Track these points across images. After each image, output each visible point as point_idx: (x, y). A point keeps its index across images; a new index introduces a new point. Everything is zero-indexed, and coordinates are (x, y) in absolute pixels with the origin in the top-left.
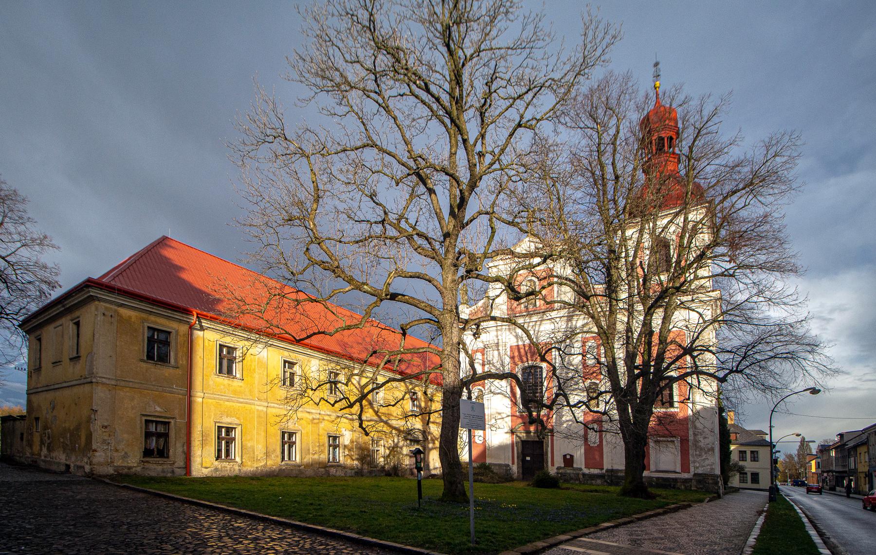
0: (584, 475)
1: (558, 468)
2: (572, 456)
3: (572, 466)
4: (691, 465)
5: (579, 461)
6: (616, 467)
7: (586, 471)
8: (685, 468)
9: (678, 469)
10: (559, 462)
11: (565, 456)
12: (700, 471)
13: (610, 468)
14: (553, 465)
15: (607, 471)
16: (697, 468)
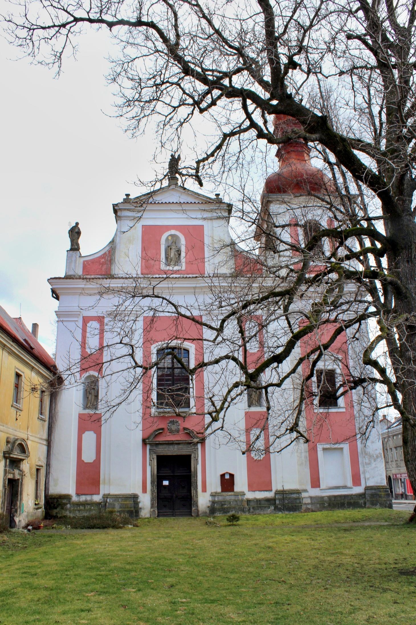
0: (249, 501)
1: (213, 495)
2: (232, 476)
3: (232, 490)
4: (362, 476)
5: (241, 484)
6: (287, 487)
7: (250, 495)
8: (356, 481)
9: (350, 483)
10: (214, 485)
11: (223, 476)
12: (371, 483)
13: (280, 488)
14: (204, 490)
15: (277, 492)
16: (368, 479)
